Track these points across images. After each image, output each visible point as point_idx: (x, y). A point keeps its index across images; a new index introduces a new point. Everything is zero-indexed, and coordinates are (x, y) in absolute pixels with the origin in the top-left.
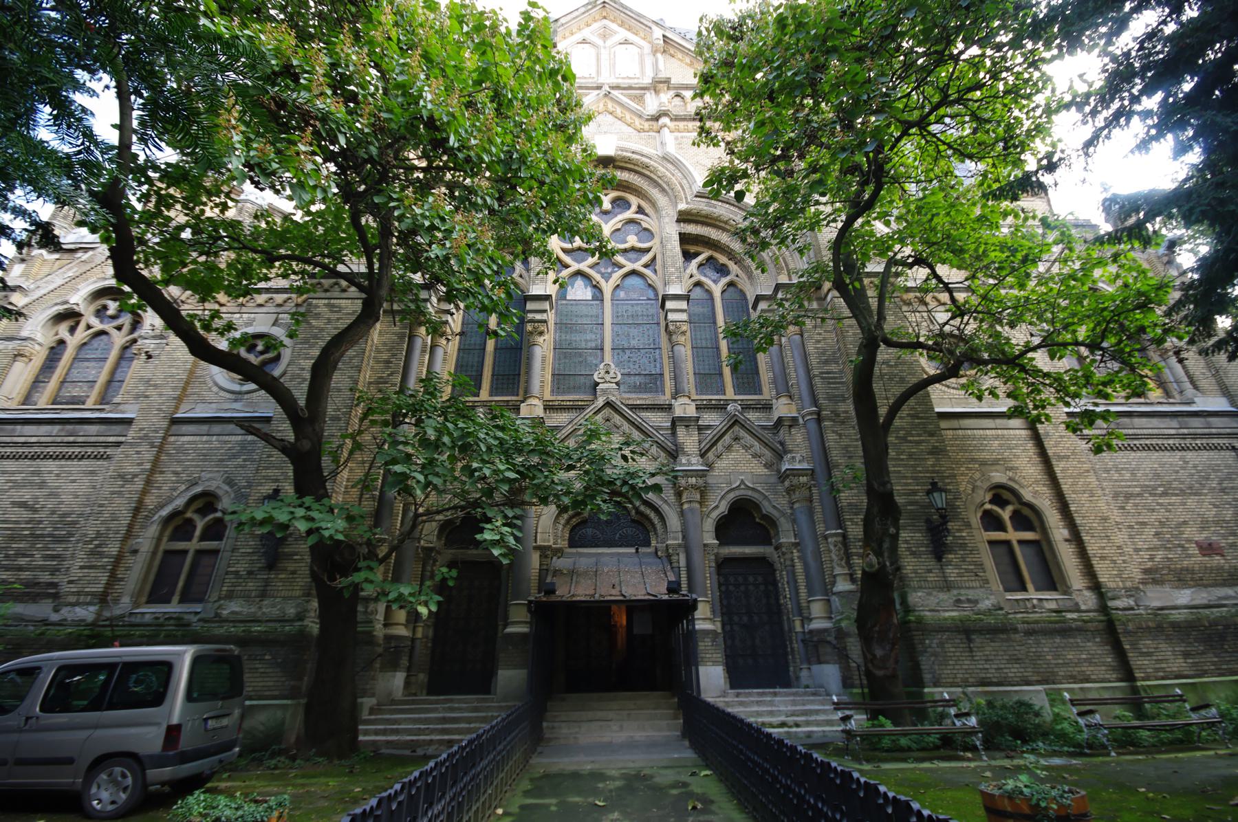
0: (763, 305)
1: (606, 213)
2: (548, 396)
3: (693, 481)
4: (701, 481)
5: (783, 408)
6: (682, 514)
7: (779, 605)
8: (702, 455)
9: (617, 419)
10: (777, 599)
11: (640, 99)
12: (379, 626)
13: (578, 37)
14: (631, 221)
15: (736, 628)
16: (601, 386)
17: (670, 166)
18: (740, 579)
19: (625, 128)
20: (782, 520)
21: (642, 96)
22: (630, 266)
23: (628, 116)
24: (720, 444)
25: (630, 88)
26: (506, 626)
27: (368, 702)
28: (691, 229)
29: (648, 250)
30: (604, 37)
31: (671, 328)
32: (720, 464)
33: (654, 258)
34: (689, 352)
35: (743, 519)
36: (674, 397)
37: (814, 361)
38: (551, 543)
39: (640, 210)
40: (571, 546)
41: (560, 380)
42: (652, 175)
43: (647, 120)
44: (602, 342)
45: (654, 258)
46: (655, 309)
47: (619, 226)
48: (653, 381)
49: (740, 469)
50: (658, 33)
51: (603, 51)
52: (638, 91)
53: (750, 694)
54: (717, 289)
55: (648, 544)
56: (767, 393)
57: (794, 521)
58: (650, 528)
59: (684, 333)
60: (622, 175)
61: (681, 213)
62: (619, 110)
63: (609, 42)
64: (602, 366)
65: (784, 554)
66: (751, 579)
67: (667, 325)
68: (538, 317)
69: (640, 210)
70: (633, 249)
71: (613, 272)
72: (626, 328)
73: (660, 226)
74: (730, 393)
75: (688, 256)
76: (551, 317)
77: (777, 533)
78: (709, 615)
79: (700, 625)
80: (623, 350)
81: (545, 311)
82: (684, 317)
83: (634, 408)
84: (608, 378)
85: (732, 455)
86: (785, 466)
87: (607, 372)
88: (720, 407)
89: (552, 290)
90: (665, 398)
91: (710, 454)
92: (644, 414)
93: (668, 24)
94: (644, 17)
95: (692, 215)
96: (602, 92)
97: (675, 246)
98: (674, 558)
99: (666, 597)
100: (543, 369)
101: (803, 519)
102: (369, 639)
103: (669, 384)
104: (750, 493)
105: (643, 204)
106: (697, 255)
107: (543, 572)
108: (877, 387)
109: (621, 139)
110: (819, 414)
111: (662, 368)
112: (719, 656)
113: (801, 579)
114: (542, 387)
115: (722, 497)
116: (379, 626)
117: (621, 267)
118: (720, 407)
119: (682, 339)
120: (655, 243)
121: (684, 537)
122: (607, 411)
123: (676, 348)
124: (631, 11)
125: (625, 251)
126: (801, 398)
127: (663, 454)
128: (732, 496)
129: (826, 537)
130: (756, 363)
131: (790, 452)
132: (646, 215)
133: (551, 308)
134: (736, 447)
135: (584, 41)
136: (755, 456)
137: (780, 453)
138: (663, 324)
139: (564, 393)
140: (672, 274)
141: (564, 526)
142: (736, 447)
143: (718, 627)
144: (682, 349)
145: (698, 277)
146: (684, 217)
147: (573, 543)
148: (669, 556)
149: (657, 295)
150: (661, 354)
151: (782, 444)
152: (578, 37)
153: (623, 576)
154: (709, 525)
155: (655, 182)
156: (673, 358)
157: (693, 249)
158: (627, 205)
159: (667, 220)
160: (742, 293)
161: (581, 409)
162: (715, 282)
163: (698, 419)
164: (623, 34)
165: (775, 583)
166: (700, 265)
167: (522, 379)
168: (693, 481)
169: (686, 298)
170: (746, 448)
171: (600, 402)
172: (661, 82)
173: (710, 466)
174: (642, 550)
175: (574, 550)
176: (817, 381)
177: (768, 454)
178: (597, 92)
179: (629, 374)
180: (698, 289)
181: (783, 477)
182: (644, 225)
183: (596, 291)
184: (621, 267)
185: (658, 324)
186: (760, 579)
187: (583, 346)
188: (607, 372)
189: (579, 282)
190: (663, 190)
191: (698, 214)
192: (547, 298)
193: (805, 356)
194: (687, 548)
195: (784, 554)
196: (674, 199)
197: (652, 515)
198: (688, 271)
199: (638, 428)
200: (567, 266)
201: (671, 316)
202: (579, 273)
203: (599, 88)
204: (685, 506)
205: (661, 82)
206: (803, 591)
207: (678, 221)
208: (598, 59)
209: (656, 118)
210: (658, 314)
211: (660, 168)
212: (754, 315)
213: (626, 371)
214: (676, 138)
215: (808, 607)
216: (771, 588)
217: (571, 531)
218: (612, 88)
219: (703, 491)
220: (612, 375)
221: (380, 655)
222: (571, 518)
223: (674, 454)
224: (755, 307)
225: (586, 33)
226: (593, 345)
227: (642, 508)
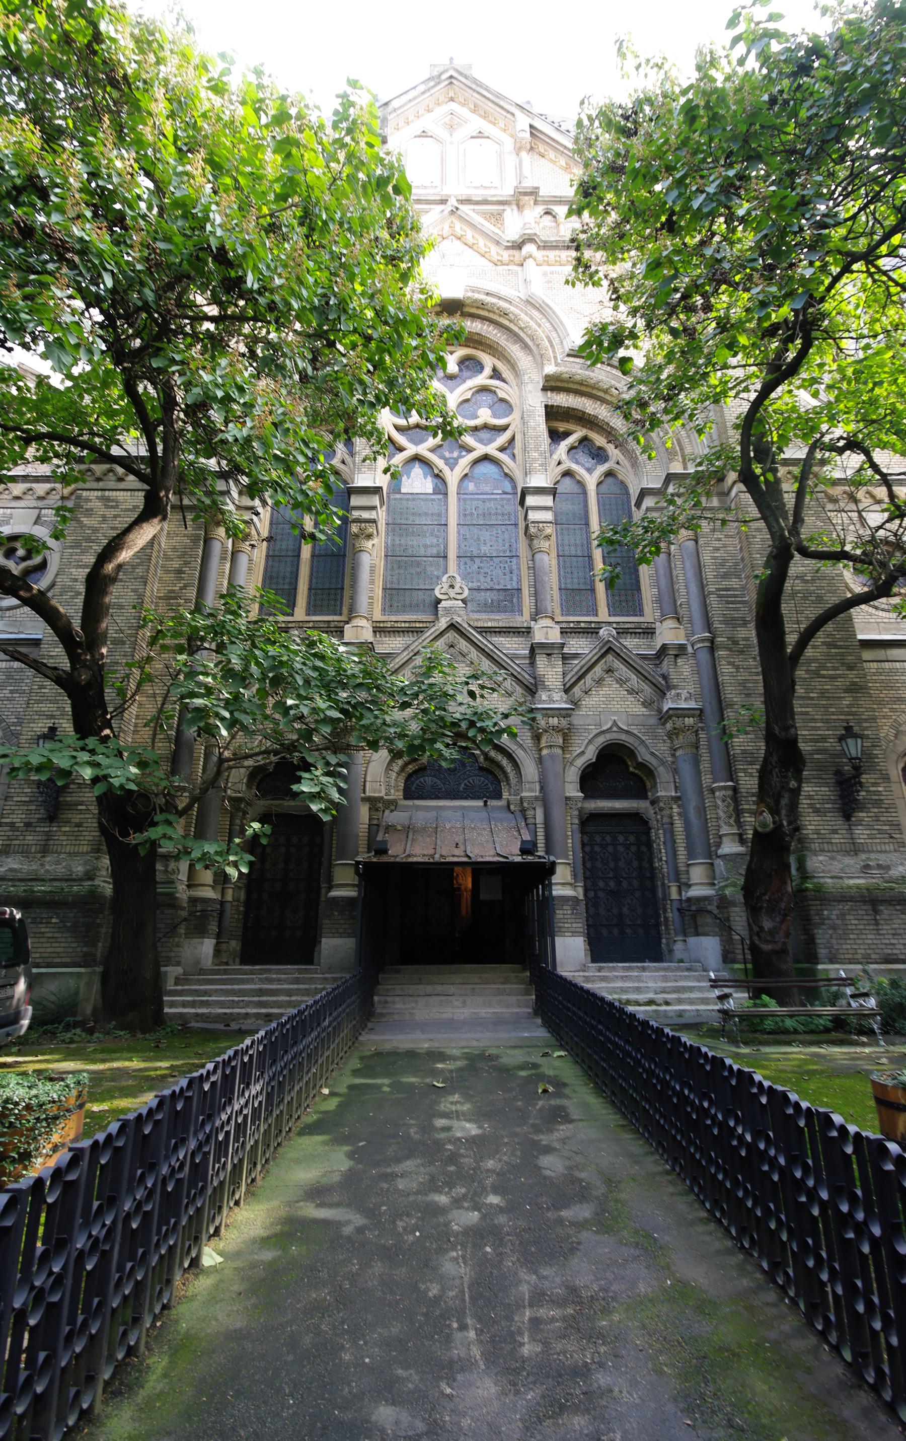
0: (649, 502)
1: (451, 377)
2: (378, 616)
3: (554, 721)
4: (564, 722)
5: (669, 633)
6: (540, 761)
7: (653, 869)
8: (566, 691)
9: (463, 644)
10: (651, 862)
11: (497, 218)
12: (182, 887)
13: (417, 127)
14: (484, 389)
15: (601, 894)
16: (443, 604)
17: (535, 313)
18: (608, 839)
20: (661, 769)
21: (500, 214)
22: (481, 450)
23: (481, 242)
24: (589, 677)
25: (485, 202)
26: (330, 888)
27: (172, 972)
28: (562, 400)
29: (505, 428)
30: (451, 127)
31: (532, 530)
32: (587, 702)
33: (513, 439)
34: (554, 562)
35: (614, 767)
36: (536, 616)
37: (709, 573)
38: (382, 794)
39: (496, 374)
40: (406, 797)
41: (394, 595)
42: (512, 326)
43: (507, 248)
44: (446, 547)
45: (513, 439)
46: (512, 506)
47: (468, 395)
48: (508, 598)
49: (611, 708)
50: (523, 122)
52: (495, 207)
53: (614, 968)
54: (591, 481)
55: (499, 796)
56: (650, 613)
57: (676, 771)
58: (501, 777)
59: (548, 537)
61: (548, 378)
62: (469, 234)
64: (444, 579)
65: (661, 809)
66: (621, 838)
67: (527, 527)
68: (366, 515)
69: (496, 374)
70: (486, 427)
72: (475, 530)
73: (521, 396)
74: (603, 614)
75: (556, 436)
76: (381, 515)
77: (655, 785)
78: (569, 879)
79: (557, 891)
80: (472, 558)
81: (374, 508)
82: (548, 516)
83: (483, 631)
84: (452, 593)
86: (668, 705)
87: (452, 587)
88: (591, 631)
89: (383, 481)
91: (577, 690)
92: (497, 640)
93: (535, 110)
94: (505, 98)
95: (562, 381)
96: (448, 208)
98: (530, 813)
99: (518, 859)
100: (372, 582)
101: (686, 769)
102: (171, 902)
103: (527, 603)
104: (623, 737)
105: (501, 366)
106: (567, 434)
107: (374, 828)
108: (786, 608)
110: (712, 641)
111: (519, 581)
112: (580, 926)
113: (680, 839)
114: (371, 604)
115: (590, 742)
116: (182, 887)
117: (470, 450)
118: (591, 631)
119: (545, 545)
120: (513, 419)
121: (542, 789)
122: (451, 635)
123: (537, 556)
124: (487, 89)
125: (476, 429)
126: (691, 622)
128: (601, 740)
129: (712, 791)
130: (638, 576)
131: (675, 687)
132: (504, 381)
133: (382, 505)
135: (424, 134)
136: (631, 692)
137: (662, 693)
138: (522, 525)
139: (398, 612)
140: (535, 460)
141: (398, 774)
142: (609, 680)
143: (580, 893)
144: (545, 557)
145: (569, 464)
146: (552, 384)
147: (408, 795)
148: (523, 811)
149: (515, 487)
150: (518, 564)
151: (665, 677)
153: (468, 834)
154: (573, 775)
155: (516, 335)
156: (534, 569)
157: (562, 427)
158: (480, 367)
159: (530, 387)
160: (623, 486)
161: (419, 631)
162: (590, 471)
163: (562, 646)
164: (476, 123)
165: (649, 844)
166: (572, 448)
167: (347, 593)
168: (554, 721)
169: (552, 492)
170: (621, 682)
171: (443, 623)
172: (525, 194)
173: (576, 704)
174: (492, 803)
175: (410, 803)
176: (713, 600)
177: (647, 689)
178: (442, 207)
179: (478, 589)
180: (567, 480)
181: (664, 718)
182: (501, 394)
184: (470, 450)
185: (516, 525)
186: (632, 839)
187: (422, 553)
188: (452, 587)
189: (417, 470)
190: (526, 347)
191: (570, 380)
192: (377, 490)
193: (699, 568)
194: (544, 800)
195: (661, 809)
196: (540, 359)
197: (505, 762)
198: (556, 457)
199: (489, 656)
200: (401, 449)
201: (533, 516)
202: (417, 458)
203: (443, 202)
204: (545, 752)
205: (525, 194)
206: (682, 852)
207: (545, 389)
209: (518, 246)
210: (516, 512)
211: (523, 316)
212: (637, 515)
214: (545, 274)
215: (687, 872)
216: (644, 849)
217: (407, 780)
218: (461, 202)
219: (567, 734)
220: (457, 589)
221: (185, 920)
222: (406, 764)
223: (532, 689)
224: (638, 505)
225: (427, 122)
226: (434, 551)
227: (493, 754)
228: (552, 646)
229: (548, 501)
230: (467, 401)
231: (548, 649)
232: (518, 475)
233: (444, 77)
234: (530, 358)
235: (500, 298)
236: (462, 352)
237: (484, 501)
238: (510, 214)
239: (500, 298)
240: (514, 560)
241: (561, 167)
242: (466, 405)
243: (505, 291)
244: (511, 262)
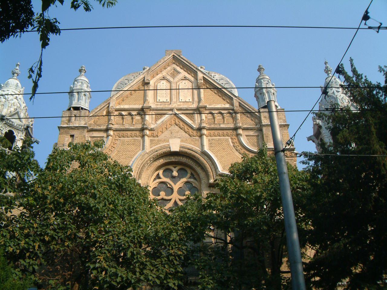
13: (160, 76)
19: (185, 133)
25: (187, 110)
60: (184, 160)
63: (176, 79)
105: (193, 172)
132: (195, 179)
135: (164, 78)
152: (160, 76)
214: (209, 140)
225: (164, 73)
234: (204, 173)
235: (193, 151)
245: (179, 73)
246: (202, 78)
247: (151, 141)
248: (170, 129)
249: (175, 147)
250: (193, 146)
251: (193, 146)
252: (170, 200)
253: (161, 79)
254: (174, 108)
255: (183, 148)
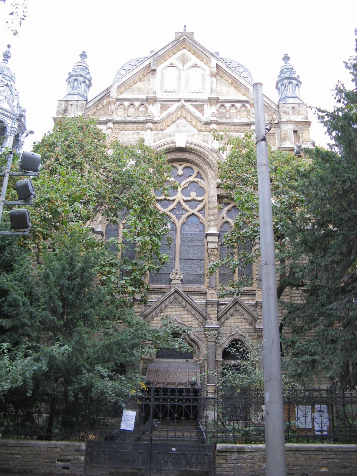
8: (218, 319)
9: (180, 299)
11: (200, 109)
16: (173, 282)
19: (192, 128)
22: (191, 211)
28: (224, 193)
29: (202, 201)
33: (205, 205)
39: (199, 175)
43: (204, 124)
50: (214, 62)
51: (182, 72)
52: (199, 104)
64: (174, 270)
69: (199, 175)
70: (193, 200)
71: (182, 214)
72: (187, 247)
80: (186, 260)
82: (216, 245)
84: (177, 277)
85: (234, 318)
90: (203, 288)
91: (223, 319)
92: (194, 297)
97: (215, 201)
104: (240, 337)
105: (200, 171)
109: (189, 136)
122: (176, 295)
125: (190, 201)
127: (200, 317)
130: (252, 269)
131: (259, 319)
132: (202, 179)
134: (236, 314)
135: (172, 65)
137: (255, 320)
140: (212, 220)
142: (236, 314)
150: (204, 263)
159: (212, 186)
164: (194, 60)
166: (229, 211)
169: (219, 235)
171: (172, 290)
172: (213, 99)
174: (190, 361)
175: (158, 359)
177: (250, 319)
179: (187, 274)
180: (226, 224)
182: (201, 185)
183: (172, 224)
184: (188, 211)
188: (177, 274)
190: (210, 167)
198: (222, 215)
207: (218, 187)
208: (179, 79)
209: (209, 123)
210: (204, 240)
211: (210, 156)
213: (186, 272)
223: (206, 318)
225: (173, 59)
228: (213, 302)
229: (216, 239)
230: (186, 187)
231: (212, 303)
232: (206, 224)
233: (181, 39)
235: (200, 147)
236: (185, 165)
237: (191, 234)
238: (207, 107)
239: (200, 147)
240: (202, 261)
241: (229, 83)
242: (185, 189)
243: (203, 144)
244: (205, 131)
245: (191, 59)
246: (215, 66)
247: (155, 135)
248: (176, 122)
249: (181, 144)
250: (201, 142)
251: (201, 142)
252: (174, 200)
253: (168, 65)
254: (181, 99)
255: (190, 144)
